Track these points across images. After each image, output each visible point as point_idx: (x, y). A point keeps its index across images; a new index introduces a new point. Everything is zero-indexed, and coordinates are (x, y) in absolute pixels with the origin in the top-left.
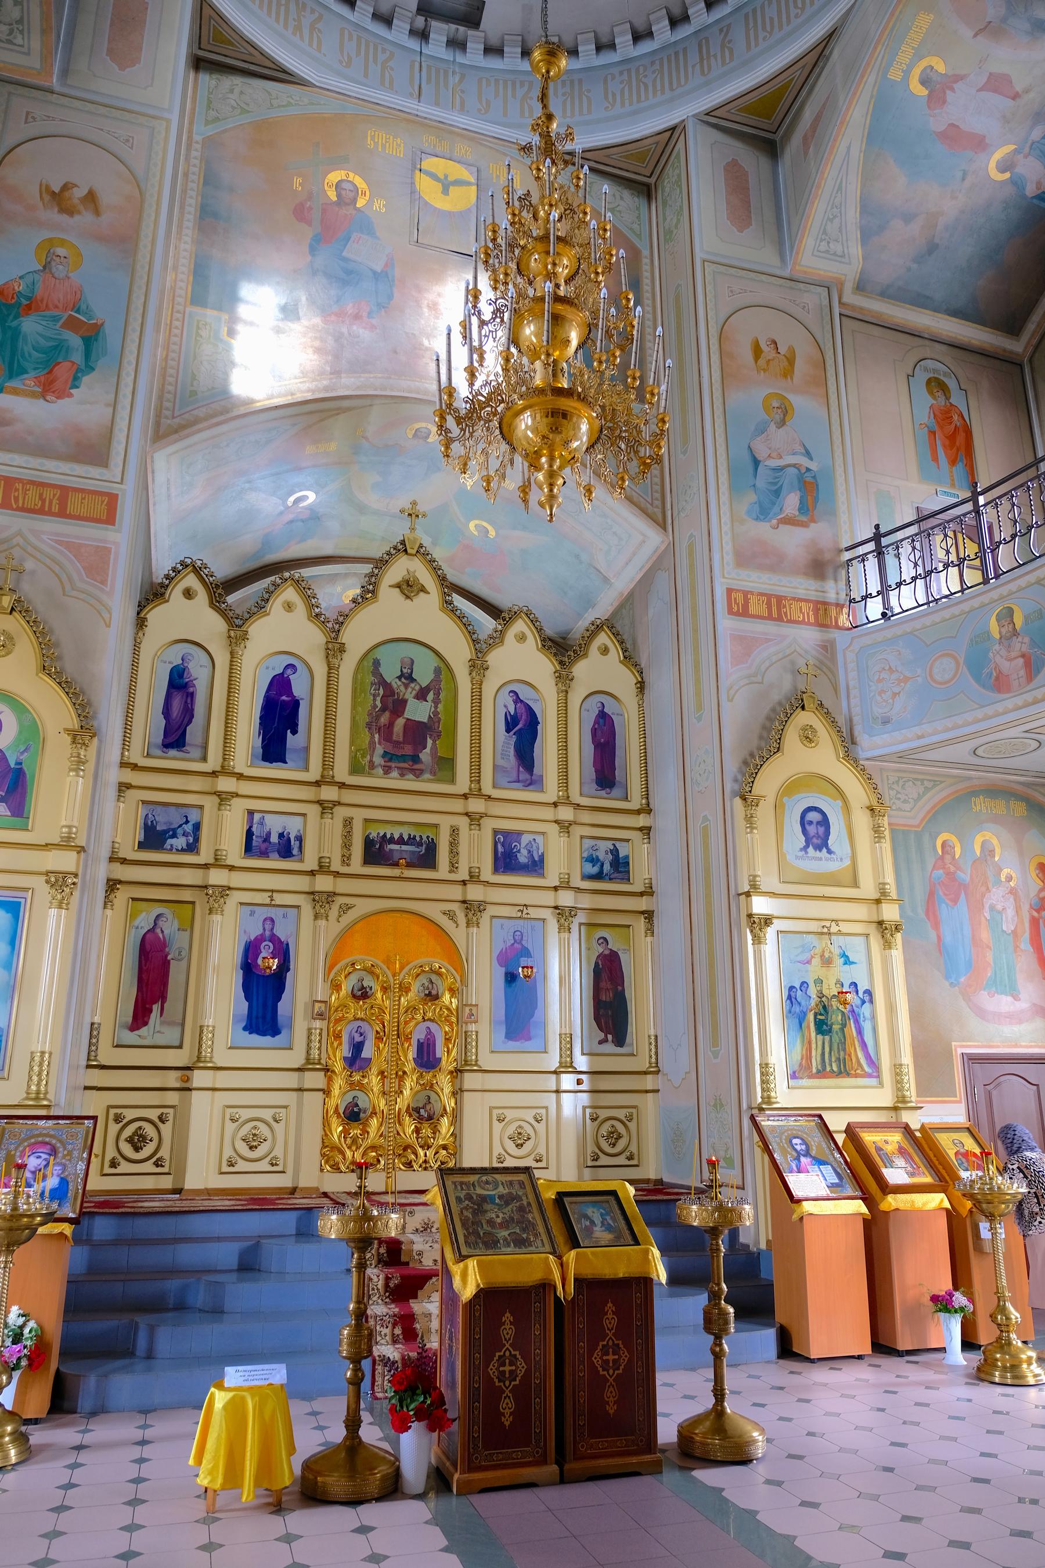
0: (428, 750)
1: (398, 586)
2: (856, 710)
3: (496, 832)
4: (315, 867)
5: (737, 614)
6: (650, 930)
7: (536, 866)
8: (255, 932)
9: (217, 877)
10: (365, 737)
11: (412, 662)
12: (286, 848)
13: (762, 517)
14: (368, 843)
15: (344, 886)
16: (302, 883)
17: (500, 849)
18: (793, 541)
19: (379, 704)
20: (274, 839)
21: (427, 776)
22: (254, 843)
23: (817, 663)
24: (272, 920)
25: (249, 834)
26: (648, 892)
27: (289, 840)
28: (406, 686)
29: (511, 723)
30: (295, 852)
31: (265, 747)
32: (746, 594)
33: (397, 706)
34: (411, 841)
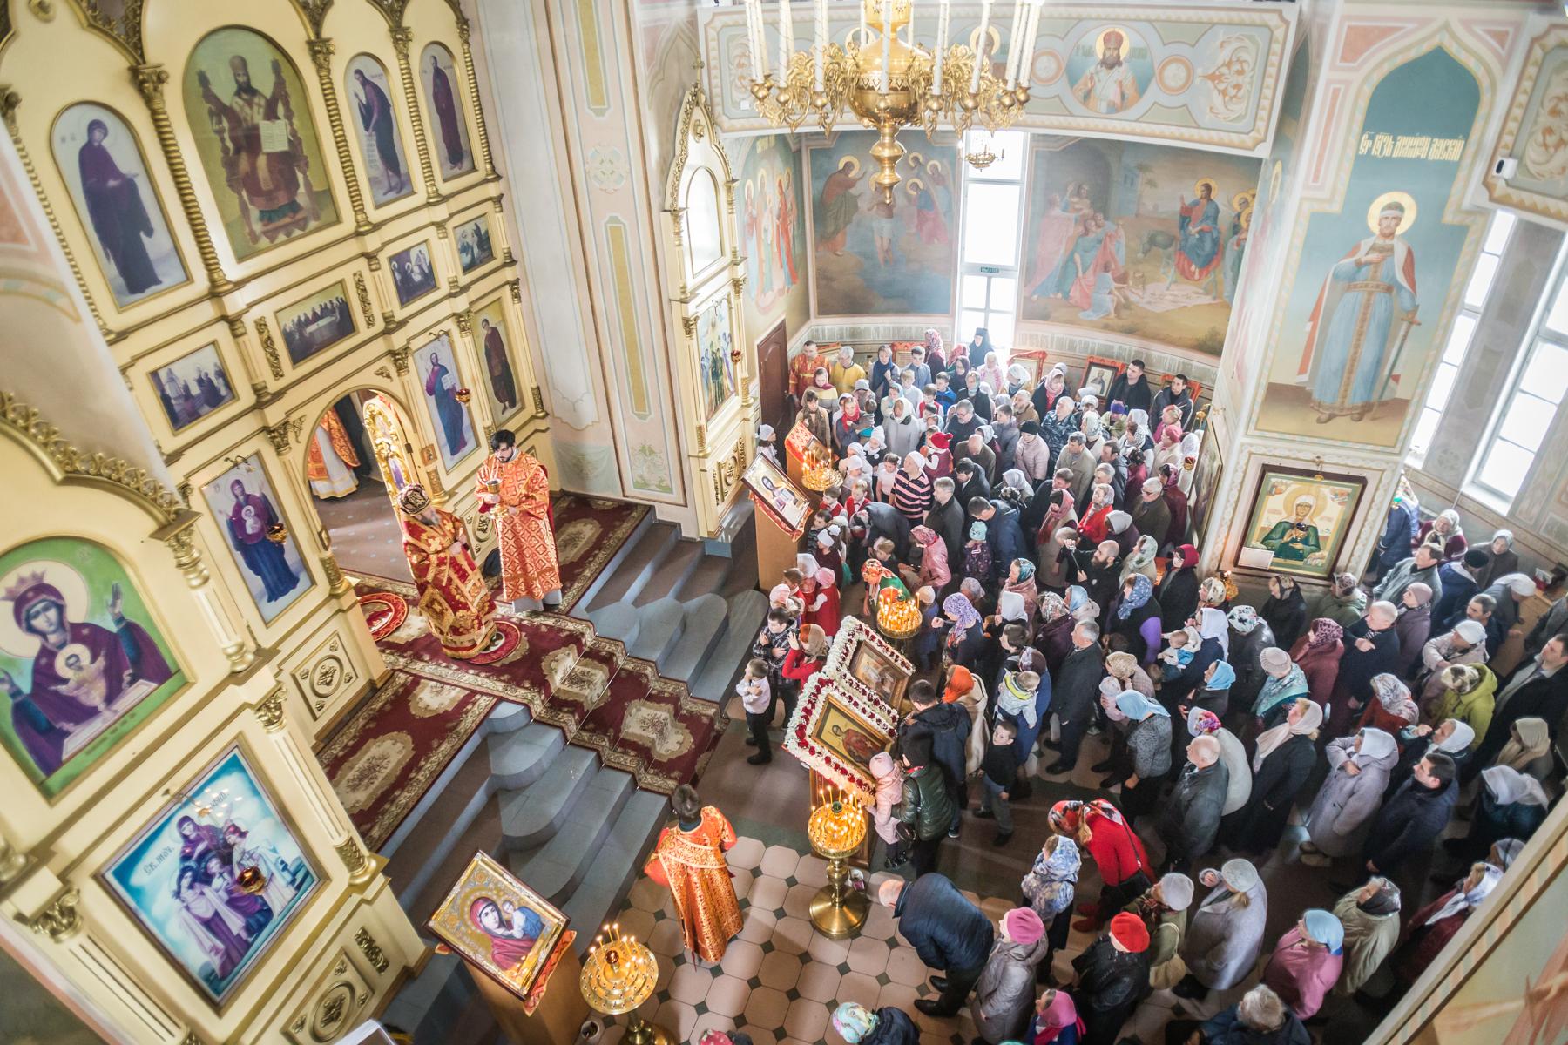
0: (302, 189)
2: (716, 91)
6: (517, 296)
7: (429, 282)
8: (228, 505)
10: (233, 199)
11: (244, 62)
12: (213, 393)
14: (288, 337)
16: (250, 423)
19: (230, 144)
20: (195, 390)
21: (313, 224)
22: (177, 409)
24: (238, 482)
25: (166, 400)
26: (511, 262)
27: (210, 381)
28: (250, 104)
30: (223, 392)
31: (124, 270)
33: (249, 141)
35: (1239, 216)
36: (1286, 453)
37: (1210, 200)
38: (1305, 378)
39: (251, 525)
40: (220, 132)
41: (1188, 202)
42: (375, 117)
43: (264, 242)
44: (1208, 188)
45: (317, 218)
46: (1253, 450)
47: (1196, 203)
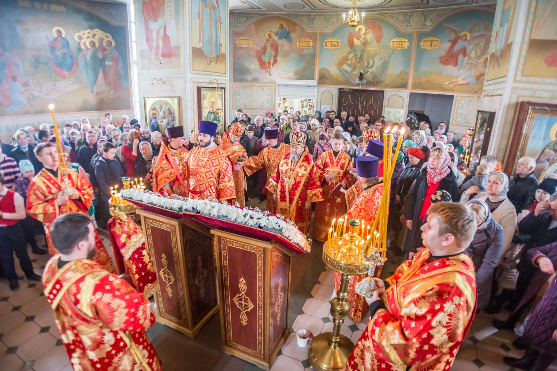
35: (79, 44)
36: (202, 80)
37: (62, 37)
38: (201, 45)
41: (51, 39)
44: (59, 32)
46: (193, 80)
47: (55, 40)
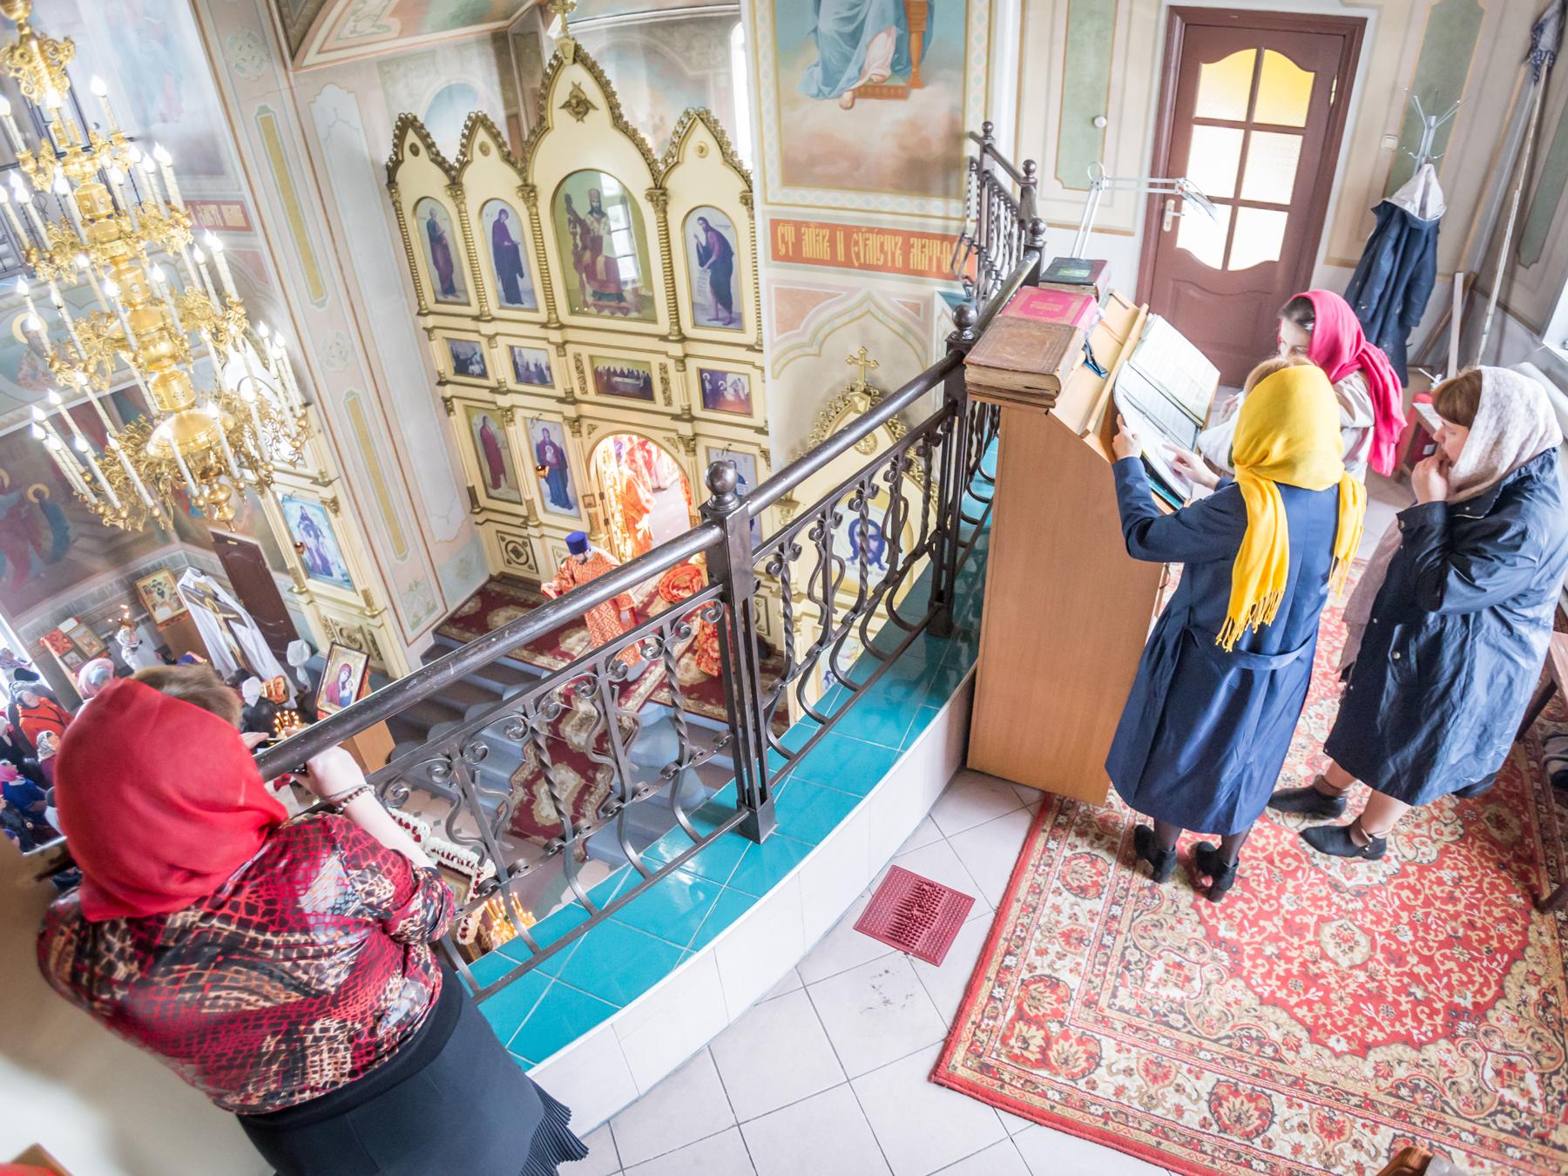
1: (563, 107)
3: (701, 371)
4: (562, 394)
5: (786, 258)
8: (540, 438)
9: (504, 401)
10: (575, 278)
13: (826, 90)
15: (586, 409)
17: (708, 386)
18: (881, 128)
20: (532, 368)
23: (900, 330)
25: (515, 364)
29: (704, 255)
31: (506, 289)
32: (798, 226)
34: (630, 375)
39: (549, 456)
40: (574, 234)
42: (713, 259)
43: (593, 310)
45: (638, 311)
